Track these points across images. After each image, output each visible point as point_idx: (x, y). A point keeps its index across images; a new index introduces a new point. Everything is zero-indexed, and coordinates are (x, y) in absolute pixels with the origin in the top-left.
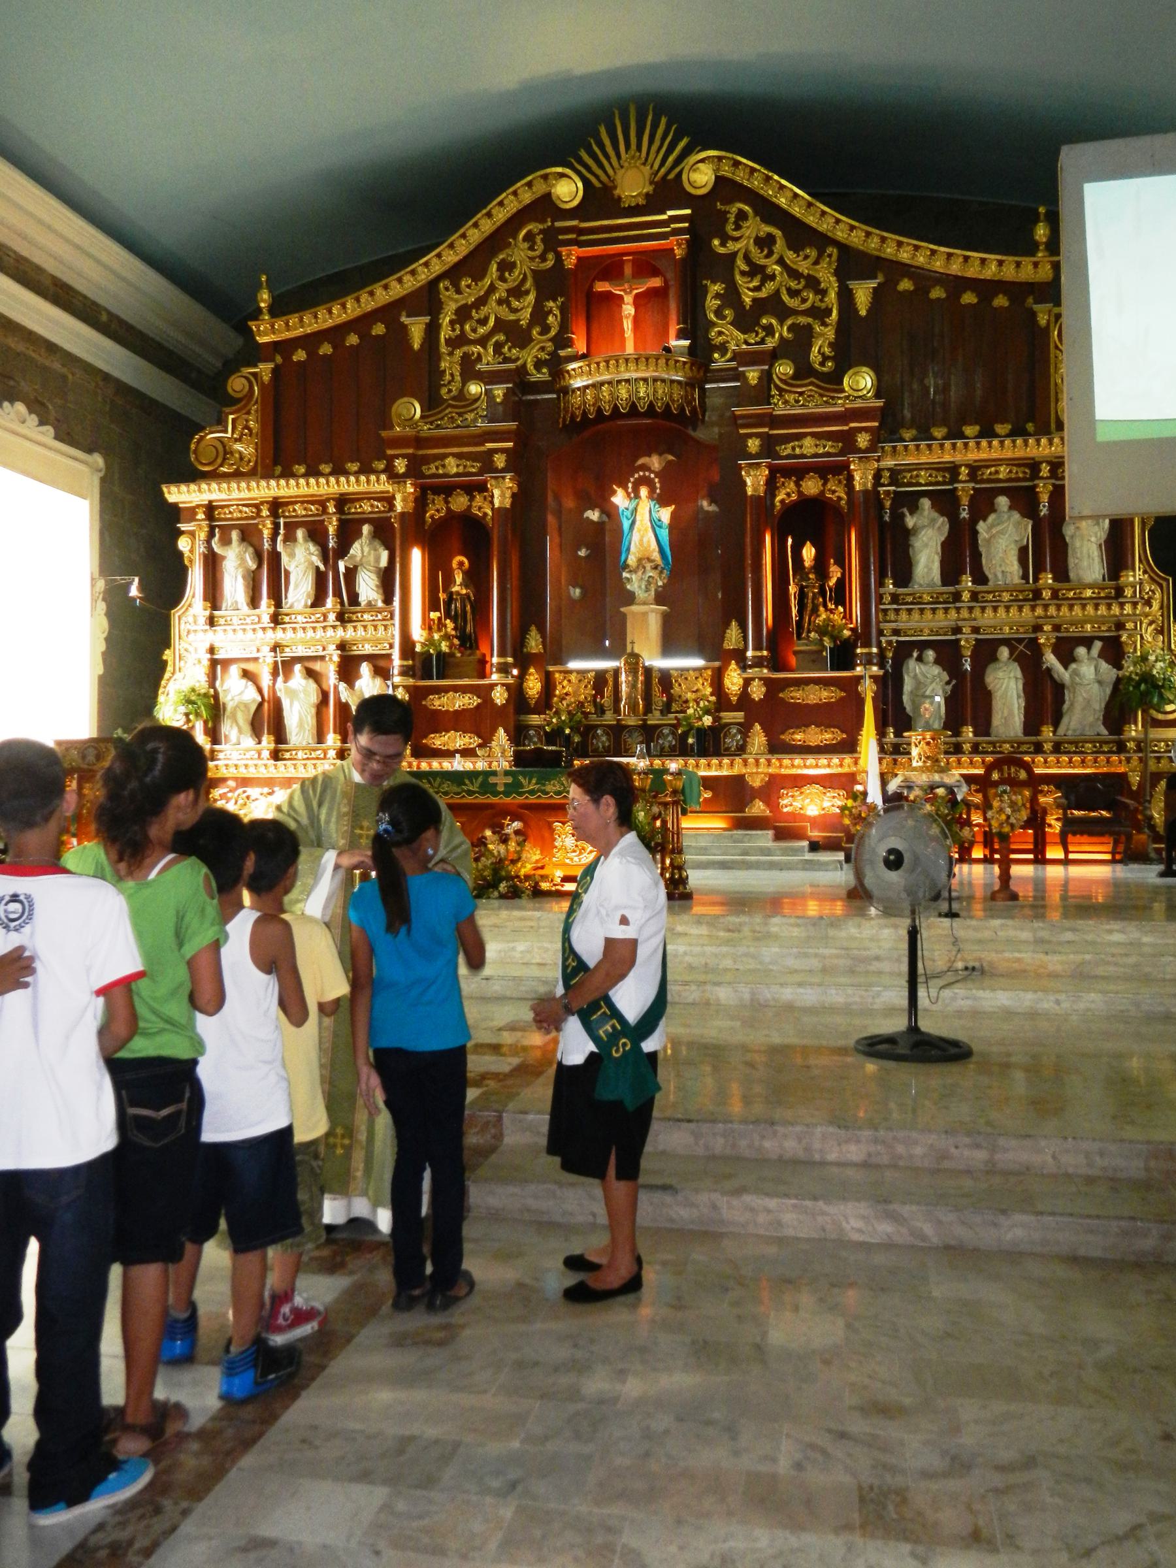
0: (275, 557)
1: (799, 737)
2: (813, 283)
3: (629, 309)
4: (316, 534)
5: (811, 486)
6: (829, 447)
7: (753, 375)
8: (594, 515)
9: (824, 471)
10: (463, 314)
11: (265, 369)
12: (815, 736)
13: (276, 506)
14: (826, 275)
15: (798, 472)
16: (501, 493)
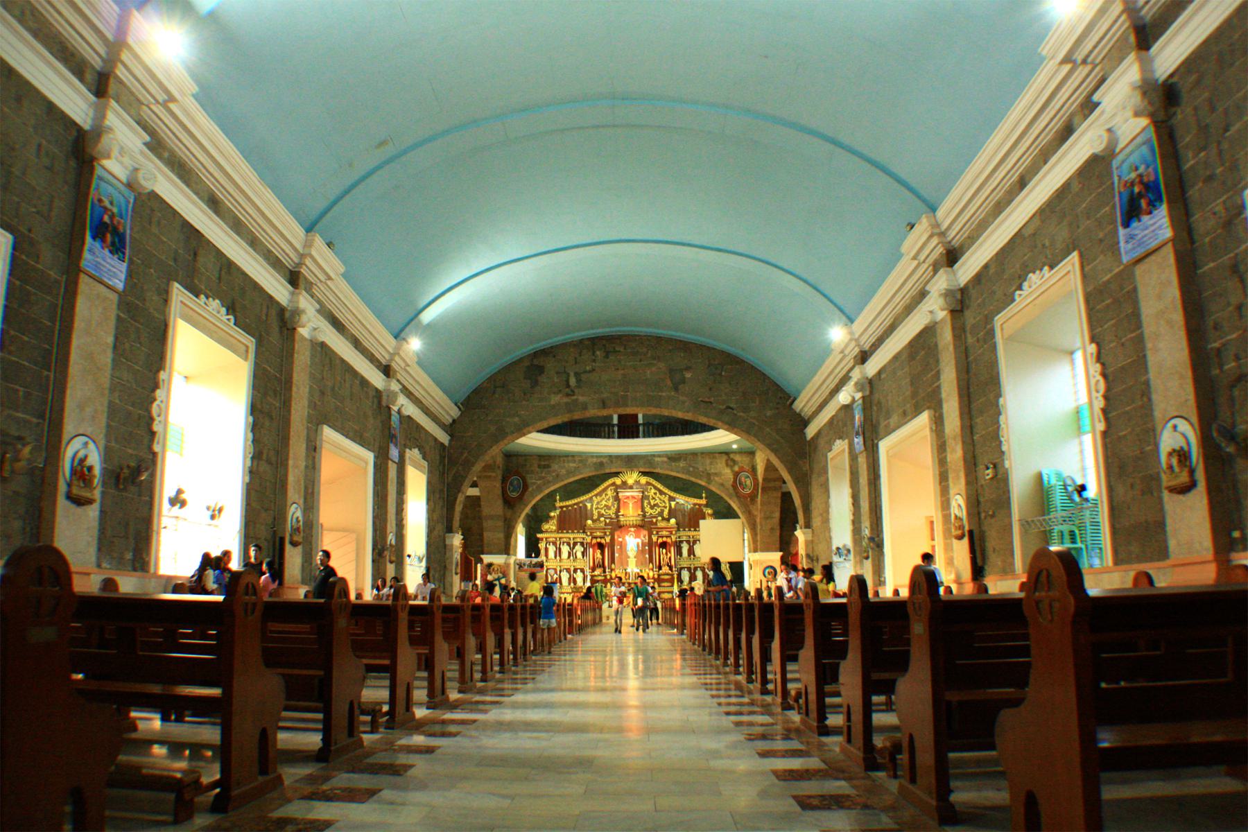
0: (560, 549)
1: (663, 584)
2: (664, 502)
3: (631, 505)
4: (569, 544)
5: (665, 539)
6: (667, 533)
7: (654, 520)
8: (620, 540)
9: (667, 537)
10: (598, 503)
11: (558, 512)
12: (666, 584)
13: (560, 538)
14: (666, 499)
15: (662, 537)
16: (608, 539)
